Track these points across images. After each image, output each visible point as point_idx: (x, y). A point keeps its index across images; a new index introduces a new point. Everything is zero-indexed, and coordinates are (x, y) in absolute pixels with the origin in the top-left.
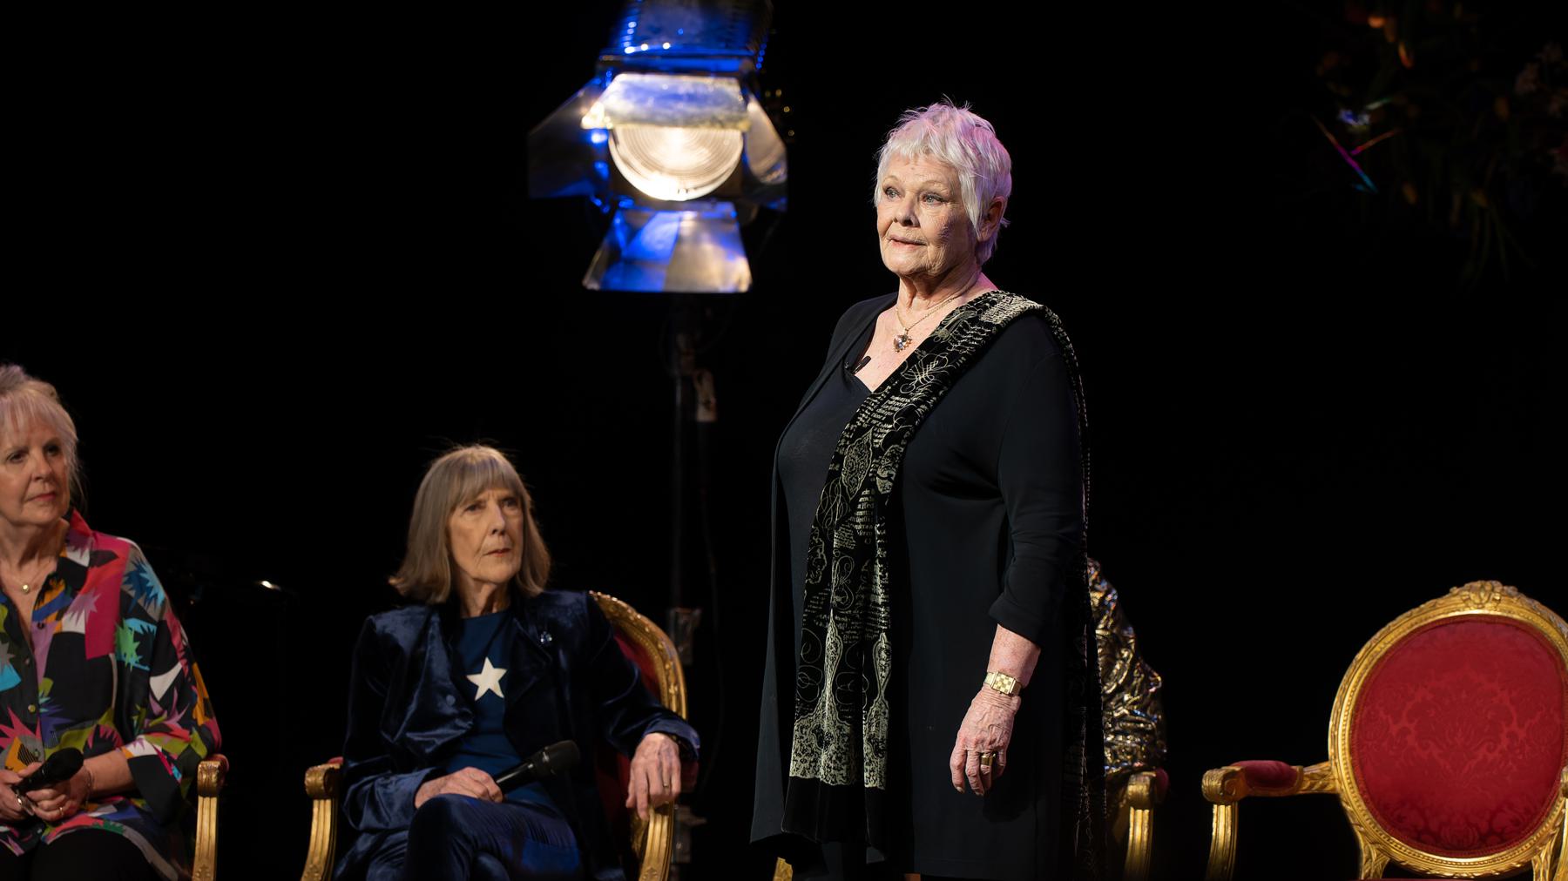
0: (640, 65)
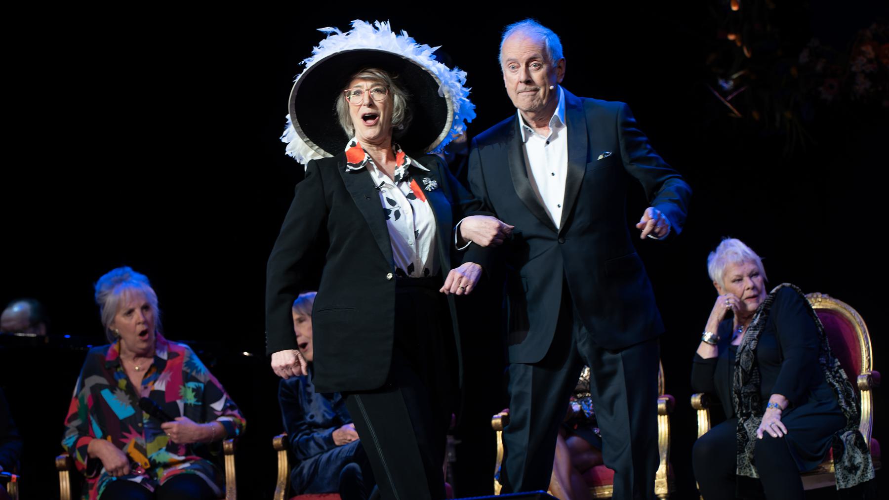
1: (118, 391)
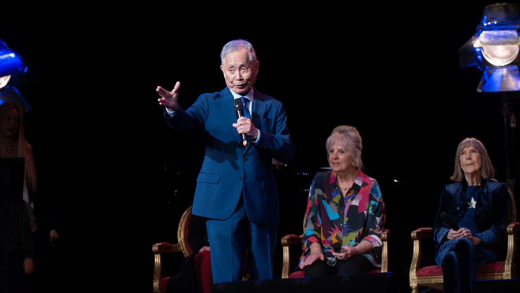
0: (489, 28)
1: (332, 203)
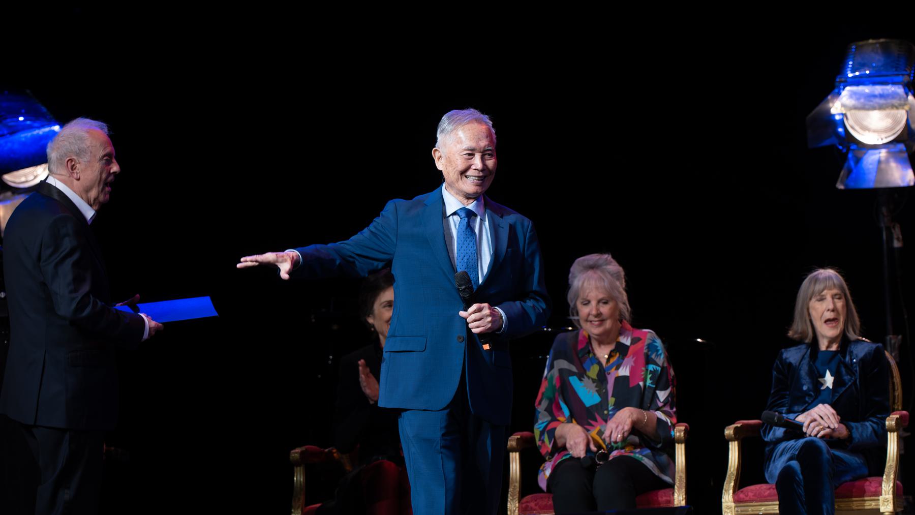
0: (856, 82)
